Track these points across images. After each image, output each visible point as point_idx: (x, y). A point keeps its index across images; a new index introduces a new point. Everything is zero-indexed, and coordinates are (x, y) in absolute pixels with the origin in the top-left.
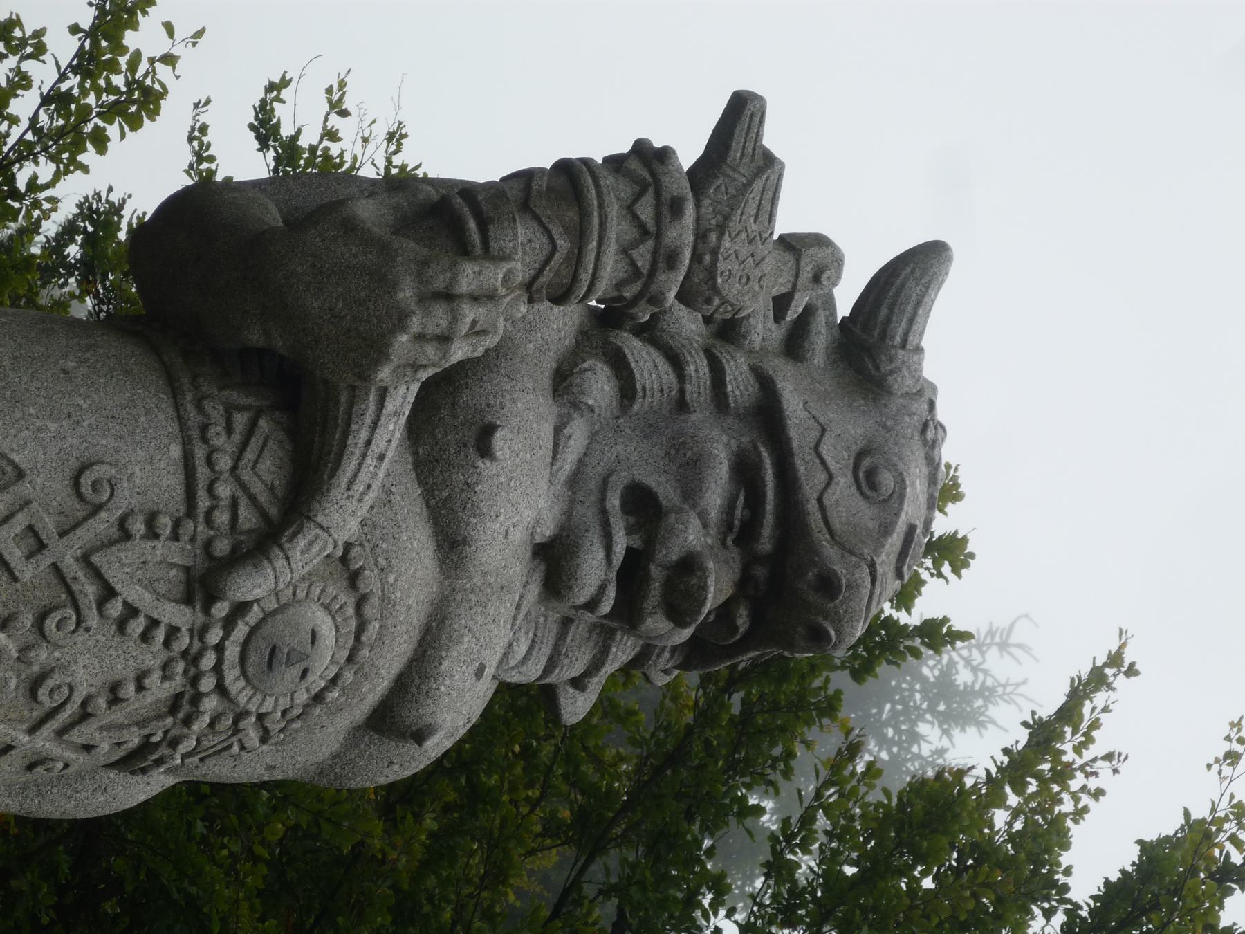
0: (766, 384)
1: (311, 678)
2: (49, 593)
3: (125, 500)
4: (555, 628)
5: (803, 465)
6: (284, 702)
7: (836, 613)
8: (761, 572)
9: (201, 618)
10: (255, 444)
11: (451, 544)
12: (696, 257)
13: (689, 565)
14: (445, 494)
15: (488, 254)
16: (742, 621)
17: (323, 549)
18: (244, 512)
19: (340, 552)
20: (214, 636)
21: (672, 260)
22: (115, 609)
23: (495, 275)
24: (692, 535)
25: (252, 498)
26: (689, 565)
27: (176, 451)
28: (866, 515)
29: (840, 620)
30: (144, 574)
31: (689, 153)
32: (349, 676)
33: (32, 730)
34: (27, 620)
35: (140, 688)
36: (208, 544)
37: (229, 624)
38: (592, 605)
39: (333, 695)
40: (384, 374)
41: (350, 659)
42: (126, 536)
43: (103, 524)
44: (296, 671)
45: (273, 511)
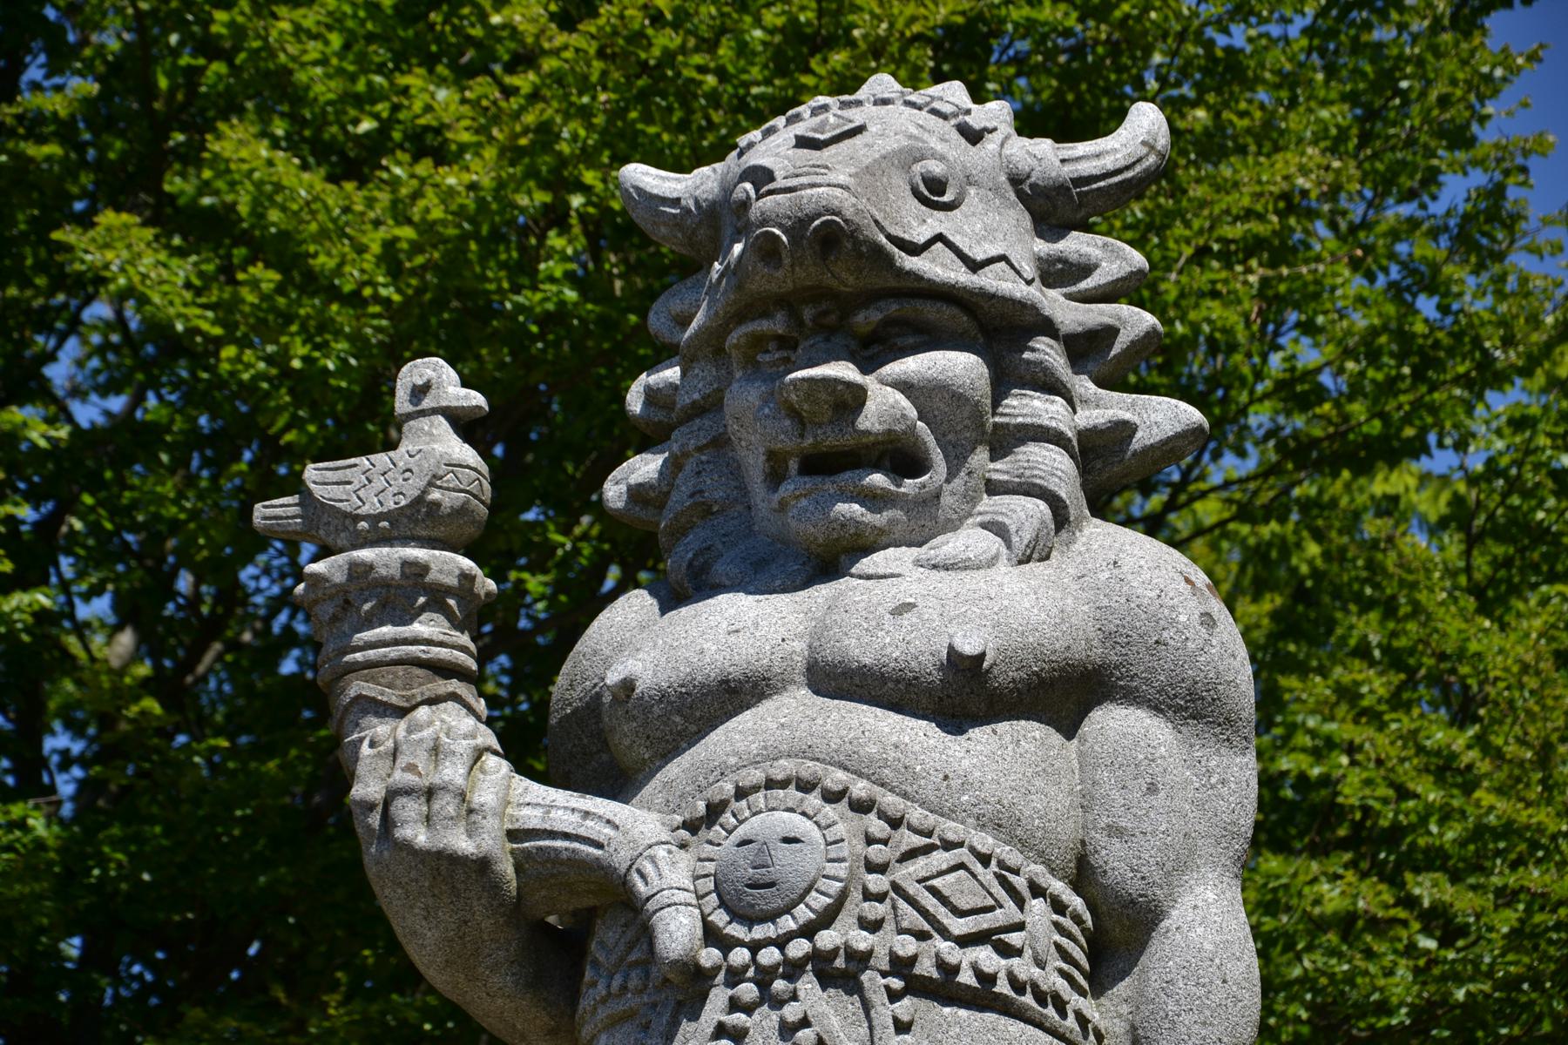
7: (793, 228)
14: (678, 719)
17: (653, 859)
18: (632, 957)
20: (740, 956)
29: (800, 220)
44: (783, 853)
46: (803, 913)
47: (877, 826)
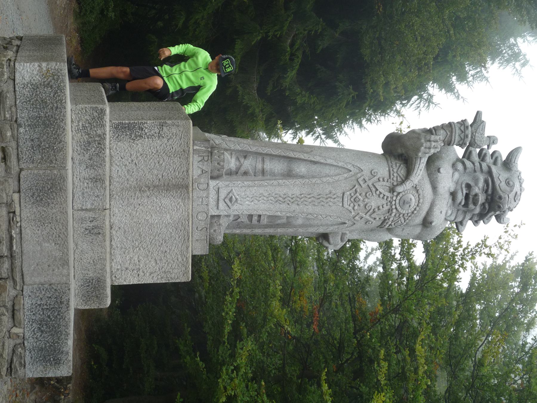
0: (489, 167)
1: (411, 207)
2: (367, 189)
3: (379, 175)
4: (456, 212)
6: (407, 212)
8: (489, 197)
9: (392, 196)
10: (400, 168)
11: (434, 188)
12: (472, 137)
13: (476, 195)
15: (436, 135)
16: (487, 206)
20: (394, 198)
21: (467, 136)
22: (378, 193)
23: (437, 138)
24: (476, 190)
25: (400, 176)
26: (476, 195)
27: (387, 169)
28: (508, 189)
30: (383, 187)
31: (470, 121)
32: (418, 208)
33: (365, 214)
34: (364, 194)
35: (383, 207)
36: (393, 183)
37: (397, 196)
38: (460, 203)
39: (415, 212)
40: (420, 154)
41: (418, 205)
42: (379, 181)
43: (375, 179)
44: (408, 205)
45: (404, 179)
46: (398, 208)
47: (409, 215)
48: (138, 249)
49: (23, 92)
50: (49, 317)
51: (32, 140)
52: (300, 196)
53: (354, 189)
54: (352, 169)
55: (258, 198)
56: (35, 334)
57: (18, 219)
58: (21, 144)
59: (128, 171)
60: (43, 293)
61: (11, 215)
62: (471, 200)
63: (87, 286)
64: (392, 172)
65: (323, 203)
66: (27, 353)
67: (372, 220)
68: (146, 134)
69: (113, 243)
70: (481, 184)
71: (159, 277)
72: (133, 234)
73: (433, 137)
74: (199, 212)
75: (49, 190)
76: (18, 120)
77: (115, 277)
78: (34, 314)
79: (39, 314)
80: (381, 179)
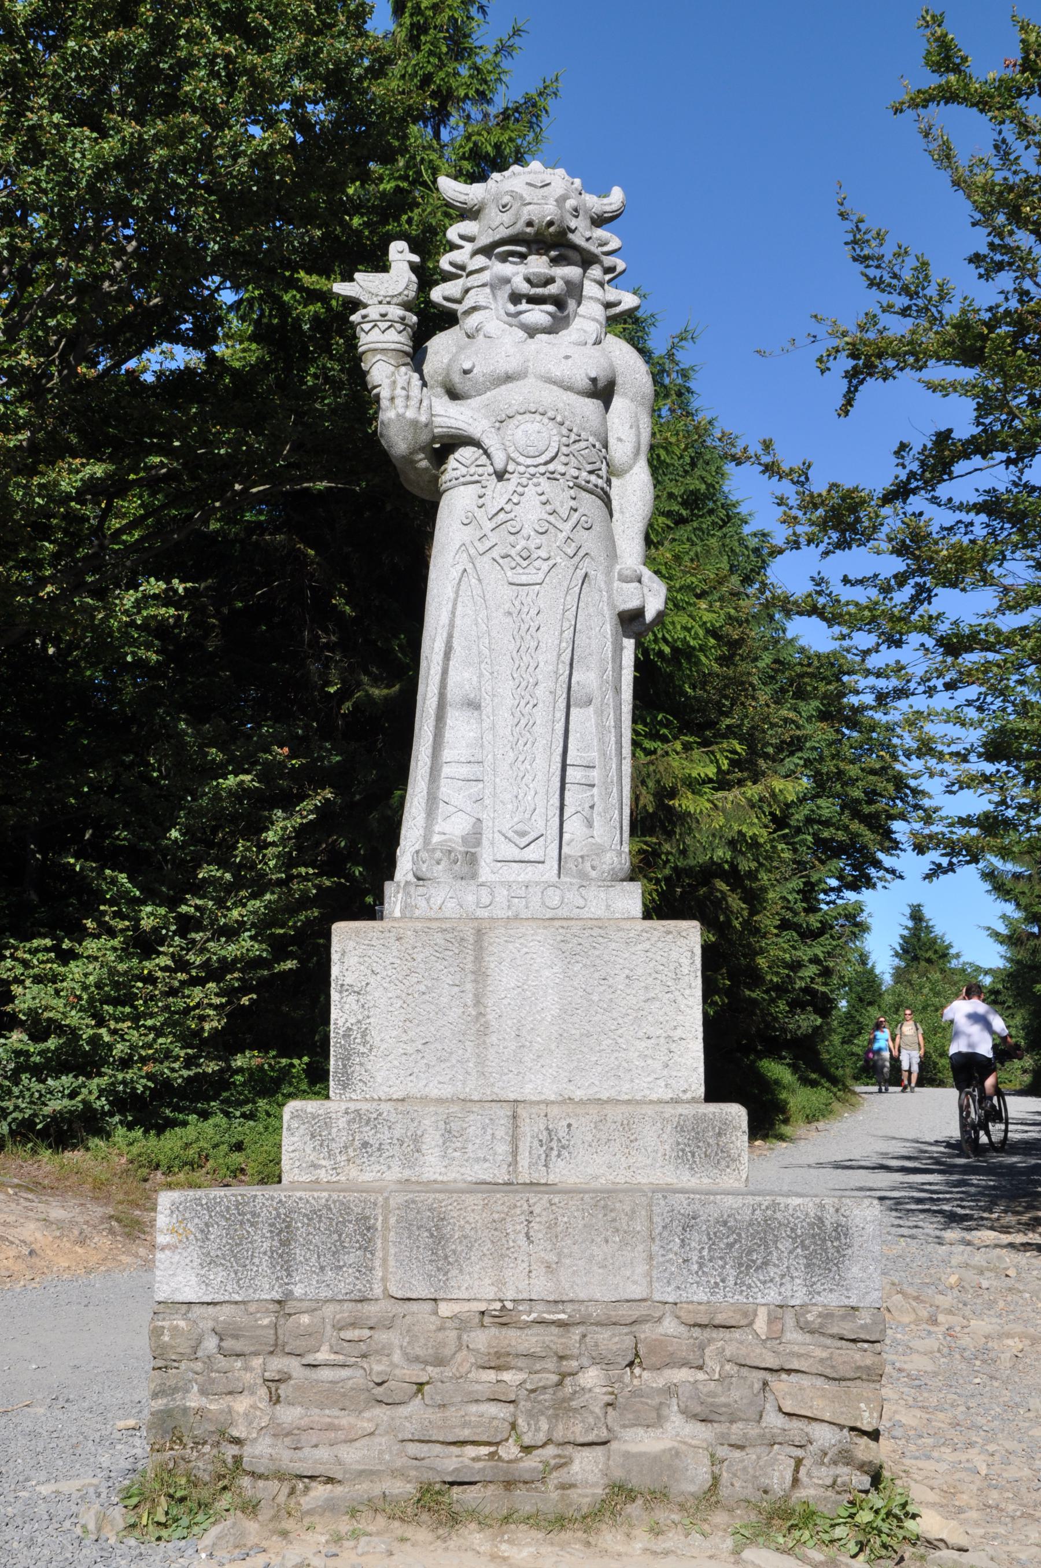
2: (503, 531)
5: (497, 237)
6: (556, 438)
8: (534, 247)
12: (389, 303)
18: (479, 463)
19: (497, 424)
20: (522, 469)
27: (462, 488)
32: (551, 414)
37: (518, 464)
39: (559, 419)
47: (565, 432)
48: (620, 1040)
49: (221, 1285)
50: (730, 1246)
51: (322, 1268)
52: (517, 682)
53: (501, 561)
54: (460, 568)
55: (521, 775)
56: (771, 1281)
57: (498, 1305)
58: (330, 1294)
59: (440, 1060)
60: (671, 1256)
61: (487, 1320)
62: (540, 291)
63: (693, 1156)
64: (468, 478)
65: (533, 630)
66: (818, 1299)
67: (575, 516)
68: (359, 1022)
69: (604, 1096)
70: (506, 269)
71: (687, 992)
72: (585, 1050)
73: (385, 393)
74: (543, 903)
75: (432, 1235)
76: (278, 1297)
77: (684, 1091)
78: (723, 1281)
79: (723, 1267)
80: (481, 501)
